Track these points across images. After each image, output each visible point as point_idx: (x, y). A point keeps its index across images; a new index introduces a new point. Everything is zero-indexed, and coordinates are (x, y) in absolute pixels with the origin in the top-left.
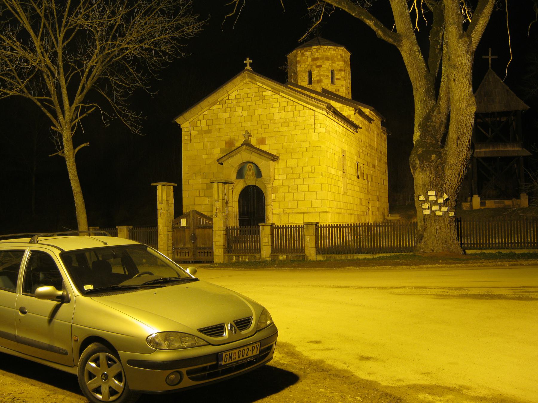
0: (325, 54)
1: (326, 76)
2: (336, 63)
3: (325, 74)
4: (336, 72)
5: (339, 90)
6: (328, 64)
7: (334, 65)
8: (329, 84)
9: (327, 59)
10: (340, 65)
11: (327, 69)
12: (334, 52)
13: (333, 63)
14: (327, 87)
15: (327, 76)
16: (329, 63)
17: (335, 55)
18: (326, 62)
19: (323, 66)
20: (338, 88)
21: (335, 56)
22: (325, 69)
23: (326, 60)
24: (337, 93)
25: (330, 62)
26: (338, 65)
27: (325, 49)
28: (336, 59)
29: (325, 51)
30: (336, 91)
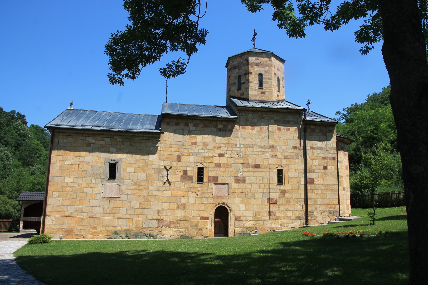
0: (234, 64)
1: (234, 84)
2: (241, 69)
3: (233, 82)
4: (242, 77)
5: (243, 93)
6: (235, 72)
7: (240, 71)
8: (236, 91)
9: (235, 68)
10: (245, 70)
11: (235, 77)
12: (240, 59)
13: (239, 69)
14: (234, 94)
15: (234, 83)
16: (236, 71)
17: (242, 61)
18: (234, 70)
19: (231, 76)
20: (243, 92)
21: (241, 63)
22: (233, 78)
23: (234, 69)
24: (242, 97)
25: (237, 70)
26: (244, 70)
27: (234, 60)
28: (242, 65)
29: (233, 62)
30: (241, 95)
